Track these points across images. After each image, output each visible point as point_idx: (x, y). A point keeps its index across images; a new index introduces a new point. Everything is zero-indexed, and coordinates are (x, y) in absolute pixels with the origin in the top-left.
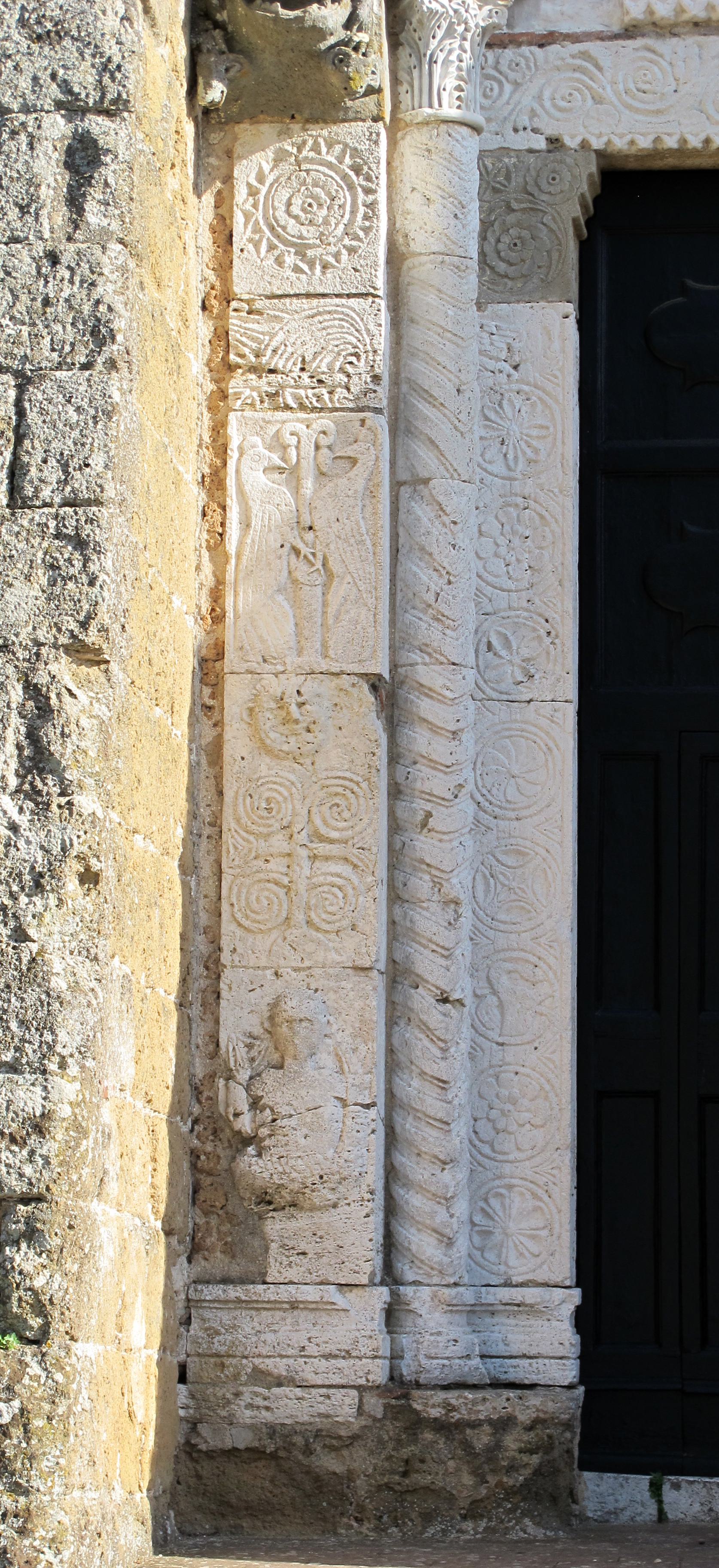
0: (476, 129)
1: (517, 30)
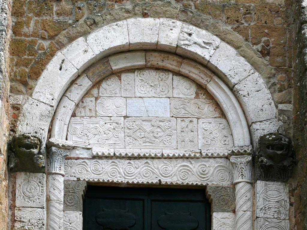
0: (63, 176)
1: (71, 156)
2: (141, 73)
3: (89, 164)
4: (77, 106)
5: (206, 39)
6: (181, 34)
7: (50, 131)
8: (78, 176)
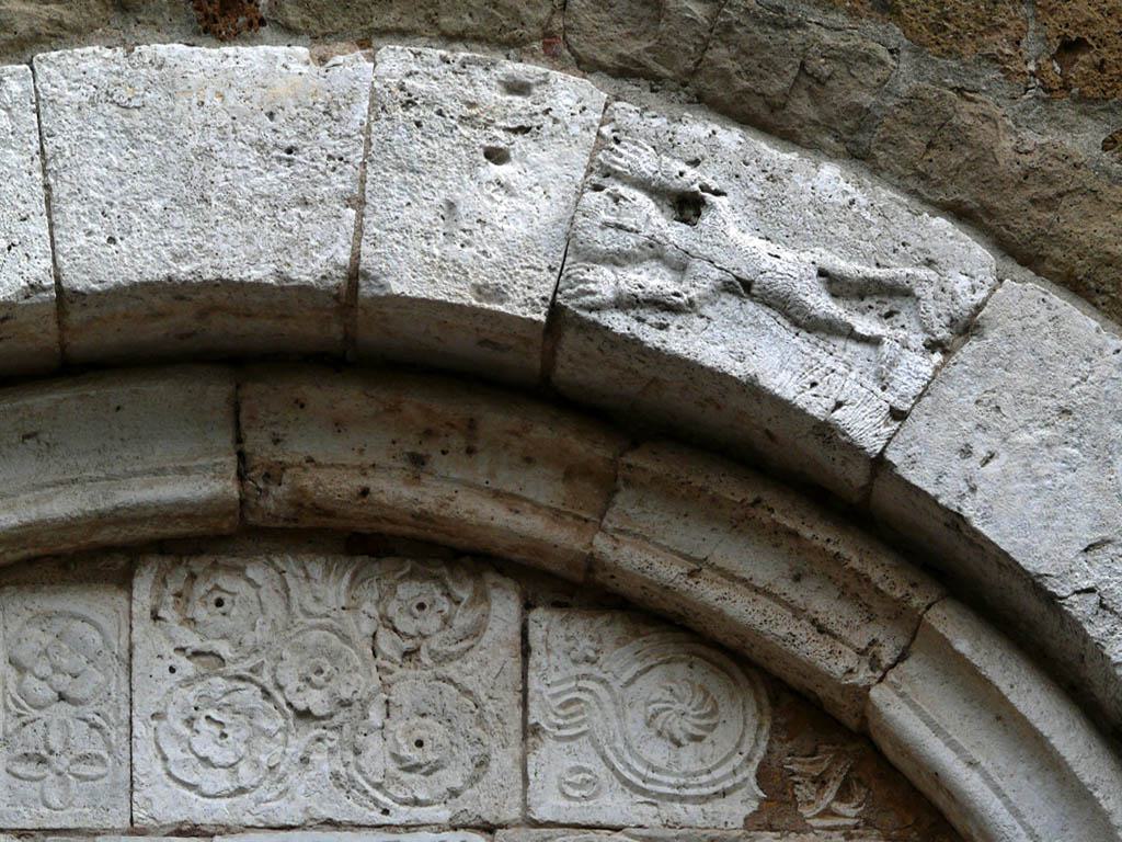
2: (201, 588)
5: (851, 250)
6: (591, 198)
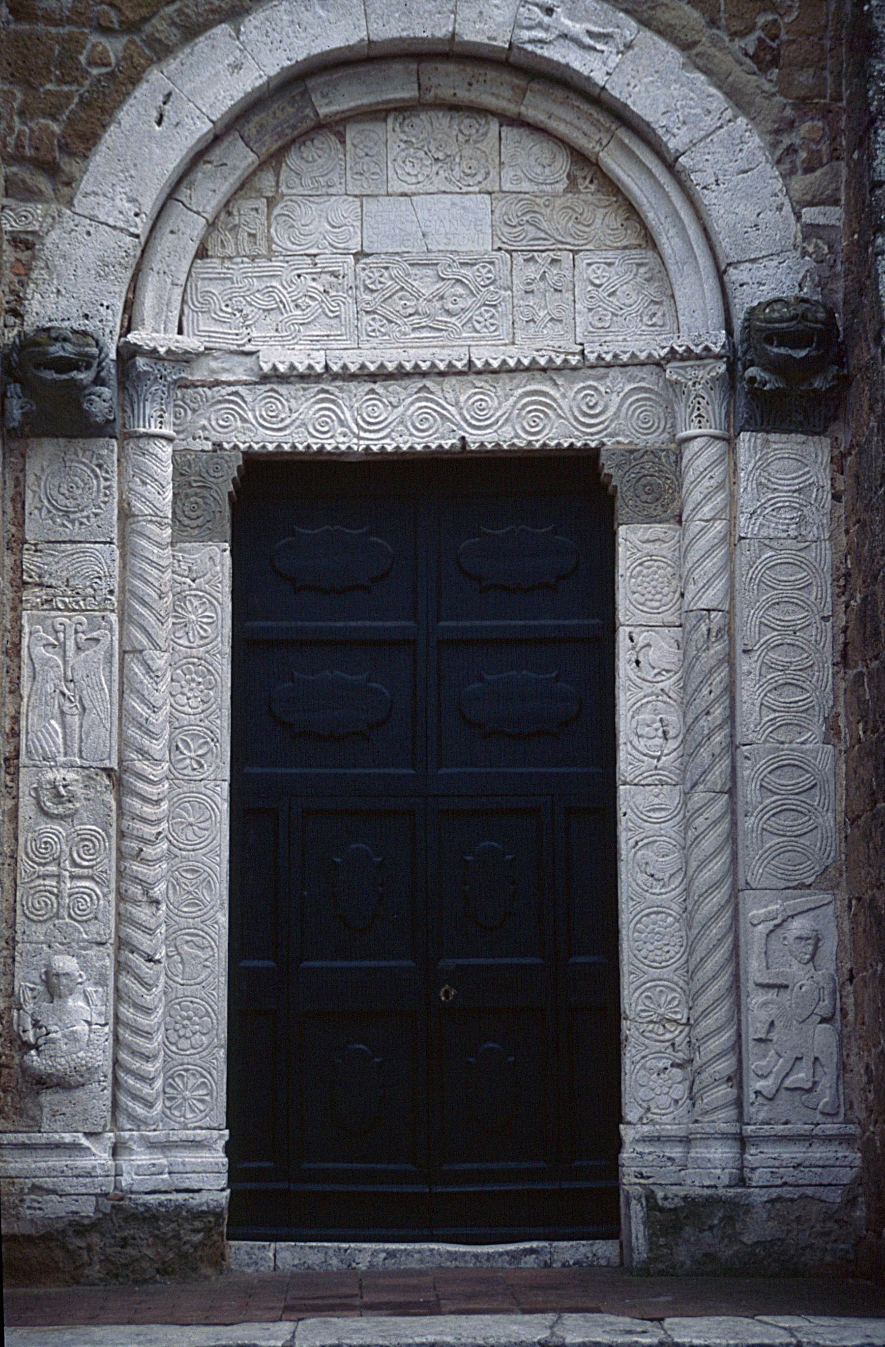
0: (170, 439)
2: (407, 122)
3: (249, 399)
4: (212, 225)
5: (595, 24)
6: (521, 9)
7: (129, 306)
8: (215, 437)
